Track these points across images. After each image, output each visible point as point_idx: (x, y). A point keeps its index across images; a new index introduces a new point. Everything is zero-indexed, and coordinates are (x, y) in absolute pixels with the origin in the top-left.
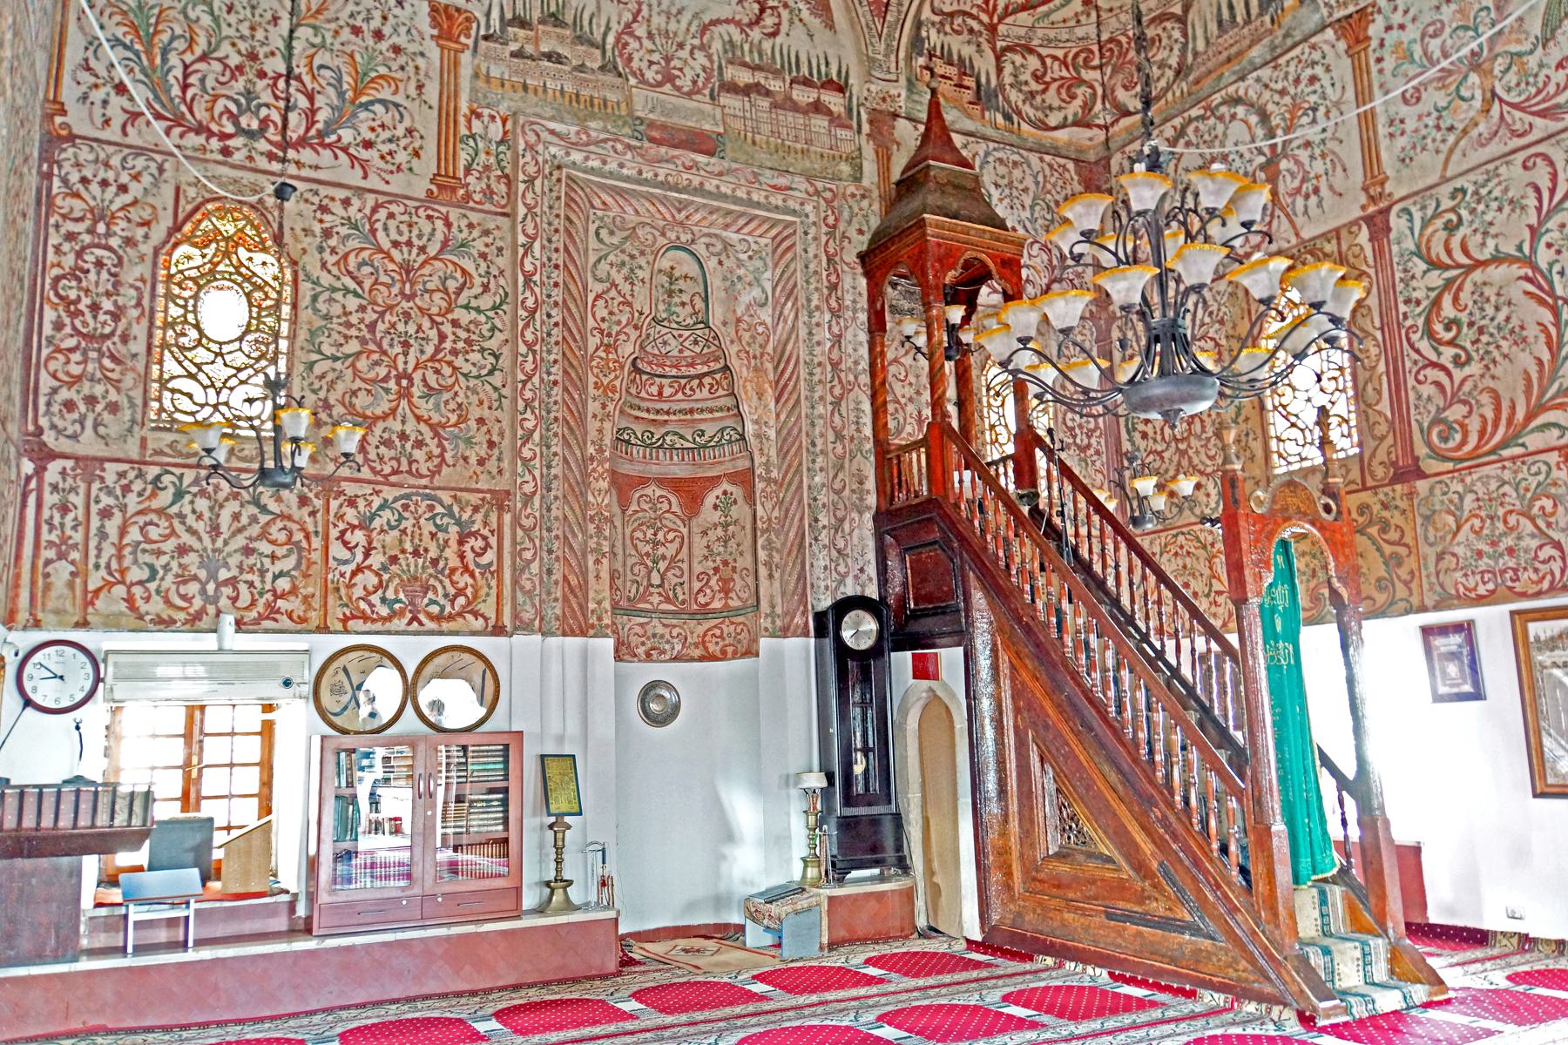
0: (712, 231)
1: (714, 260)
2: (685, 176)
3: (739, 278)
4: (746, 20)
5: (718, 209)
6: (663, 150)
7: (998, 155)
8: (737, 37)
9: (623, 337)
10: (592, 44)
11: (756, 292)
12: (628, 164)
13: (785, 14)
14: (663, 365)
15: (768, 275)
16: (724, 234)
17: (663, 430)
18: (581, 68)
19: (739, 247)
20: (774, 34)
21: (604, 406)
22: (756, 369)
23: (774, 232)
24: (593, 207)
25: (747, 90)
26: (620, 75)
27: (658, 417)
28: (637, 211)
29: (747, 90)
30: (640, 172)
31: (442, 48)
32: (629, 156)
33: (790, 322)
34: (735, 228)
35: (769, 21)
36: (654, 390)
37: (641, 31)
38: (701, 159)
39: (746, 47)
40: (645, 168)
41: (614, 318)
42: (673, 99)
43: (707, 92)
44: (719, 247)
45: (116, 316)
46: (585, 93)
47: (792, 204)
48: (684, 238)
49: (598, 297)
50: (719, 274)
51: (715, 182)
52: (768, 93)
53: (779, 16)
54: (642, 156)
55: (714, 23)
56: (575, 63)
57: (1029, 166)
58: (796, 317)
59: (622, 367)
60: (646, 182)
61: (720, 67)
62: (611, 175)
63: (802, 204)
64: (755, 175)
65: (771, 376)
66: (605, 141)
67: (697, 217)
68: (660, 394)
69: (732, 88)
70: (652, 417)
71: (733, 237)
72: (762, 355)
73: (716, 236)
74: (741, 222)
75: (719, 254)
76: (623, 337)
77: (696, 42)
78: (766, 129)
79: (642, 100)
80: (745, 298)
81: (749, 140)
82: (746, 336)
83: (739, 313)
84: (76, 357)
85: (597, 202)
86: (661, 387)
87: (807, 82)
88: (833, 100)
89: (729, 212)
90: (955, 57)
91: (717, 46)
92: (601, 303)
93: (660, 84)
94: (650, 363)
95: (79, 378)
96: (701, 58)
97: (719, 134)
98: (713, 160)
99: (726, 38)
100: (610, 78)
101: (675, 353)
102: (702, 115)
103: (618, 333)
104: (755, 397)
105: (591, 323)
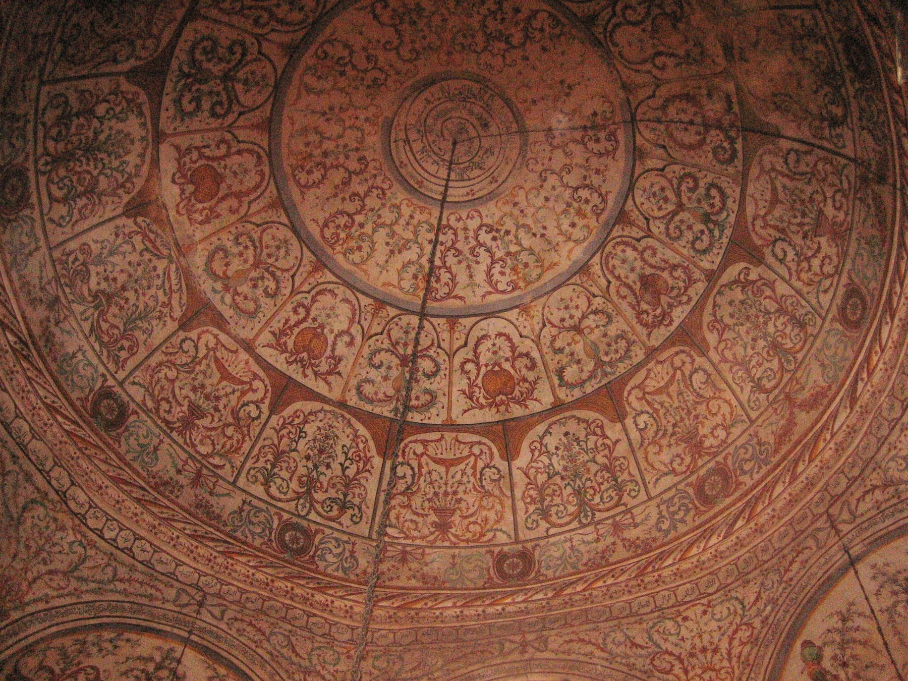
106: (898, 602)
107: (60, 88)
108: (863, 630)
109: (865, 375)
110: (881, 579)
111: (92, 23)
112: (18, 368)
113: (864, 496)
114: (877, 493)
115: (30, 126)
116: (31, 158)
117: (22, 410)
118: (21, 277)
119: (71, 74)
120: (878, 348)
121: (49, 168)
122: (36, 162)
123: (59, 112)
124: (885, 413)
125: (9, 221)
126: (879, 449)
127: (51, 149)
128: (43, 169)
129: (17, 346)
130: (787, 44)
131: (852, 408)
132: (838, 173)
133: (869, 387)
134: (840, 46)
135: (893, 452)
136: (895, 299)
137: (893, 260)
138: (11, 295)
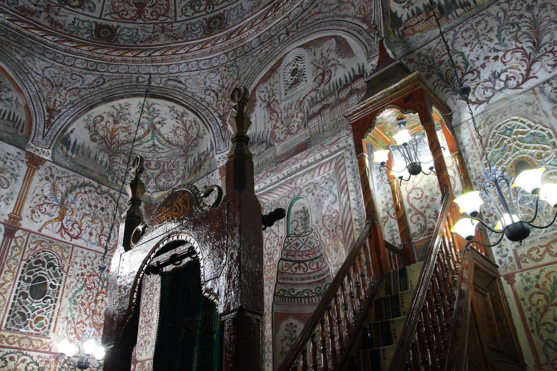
0: (308, 182)
1: (310, 195)
2: (293, 167)
3: (323, 196)
4: (317, 85)
5: (306, 172)
6: (284, 163)
7: (462, 29)
8: (313, 94)
9: (276, 252)
10: (263, 142)
11: (331, 198)
12: (272, 178)
13: (333, 69)
14: (314, 253)
15: (335, 187)
16: (313, 180)
17: (324, 284)
18: (259, 154)
19: (321, 182)
20: (329, 81)
21: (270, 287)
22: (334, 237)
23: (333, 165)
24: (264, 203)
25: (319, 112)
26: (272, 146)
27: (320, 278)
28: (278, 195)
29: (319, 112)
30: (278, 178)
31: (221, 180)
32: (272, 174)
33: (344, 204)
34: (316, 175)
35: (327, 77)
36: (315, 266)
37: (279, 124)
38: (298, 156)
39: (318, 96)
40: (279, 175)
41: (272, 245)
42: (290, 140)
43: (303, 126)
44: (312, 187)
45: (151, 313)
46: (260, 162)
47: (341, 145)
48: (296, 194)
49: (267, 239)
50: (313, 200)
51: (305, 161)
52: (328, 105)
53: (331, 71)
54: (277, 171)
55: (304, 98)
56: (257, 154)
57: (489, 15)
58: (349, 197)
59: (275, 267)
60: (281, 180)
61: (308, 112)
62: (269, 186)
63: (347, 142)
64: (322, 146)
65: (341, 237)
66: (264, 175)
67: (299, 181)
68: (318, 267)
69: (314, 115)
70: (317, 280)
71: (317, 179)
72: (336, 228)
73: (310, 183)
74: (317, 170)
75: (312, 191)
76: (276, 252)
77: (298, 111)
78: (328, 122)
79: (279, 149)
80: (326, 204)
81: (321, 132)
82: (327, 223)
83: (324, 213)
84: (144, 330)
85: (264, 201)
86: (317, 264)
87: (345, 86)
88: (358, 84)
89: (311, 170)
90: (422, 9)
91: (307, 104)
92: (268, 241)
93: (285, 138)
94: (308, 255)
95: (143, 336)
96: (300, 115)
97: (309, 139)
98: (303, 152)
99: (310, 99)
100: (269, 149)
101: (316, 245)
102: (301, 136)
103: (274, 252)
104: (334, 252)
105: (265, 252)
107: (179, 11)
111: (150, 7)
112: (282, 8)
115: (193, 21)
116: (205, 17)
117: (299, 3)
118: (248, 13)
119: (173, 8)
121: (211, 6)
122: (208, 13)
123: (189, 8)
125: (226, 23)
127: (204, 7)
128: (211, 9)
129: (273, 10)
138: (253, 17)
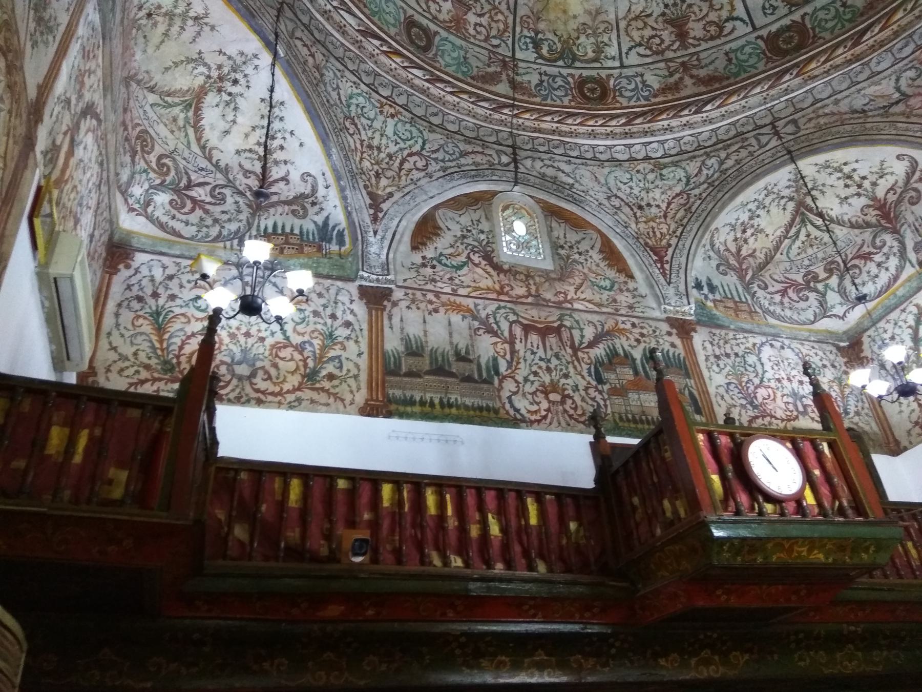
106: (209, 68)
108: (180, 34)
109: (385, 48)
110: (239, 60)
113: (305, 45)
114: (310, 60)
120: (406, 64)
124: (362, 66)
126: (337, 59)
130: (587, 19)
131: (358, 31)
132: (500, 36)
133: (377, 51)
134: (594, 73)
135: (339, 74)
136: (442, 86)
137: (470, 88)
